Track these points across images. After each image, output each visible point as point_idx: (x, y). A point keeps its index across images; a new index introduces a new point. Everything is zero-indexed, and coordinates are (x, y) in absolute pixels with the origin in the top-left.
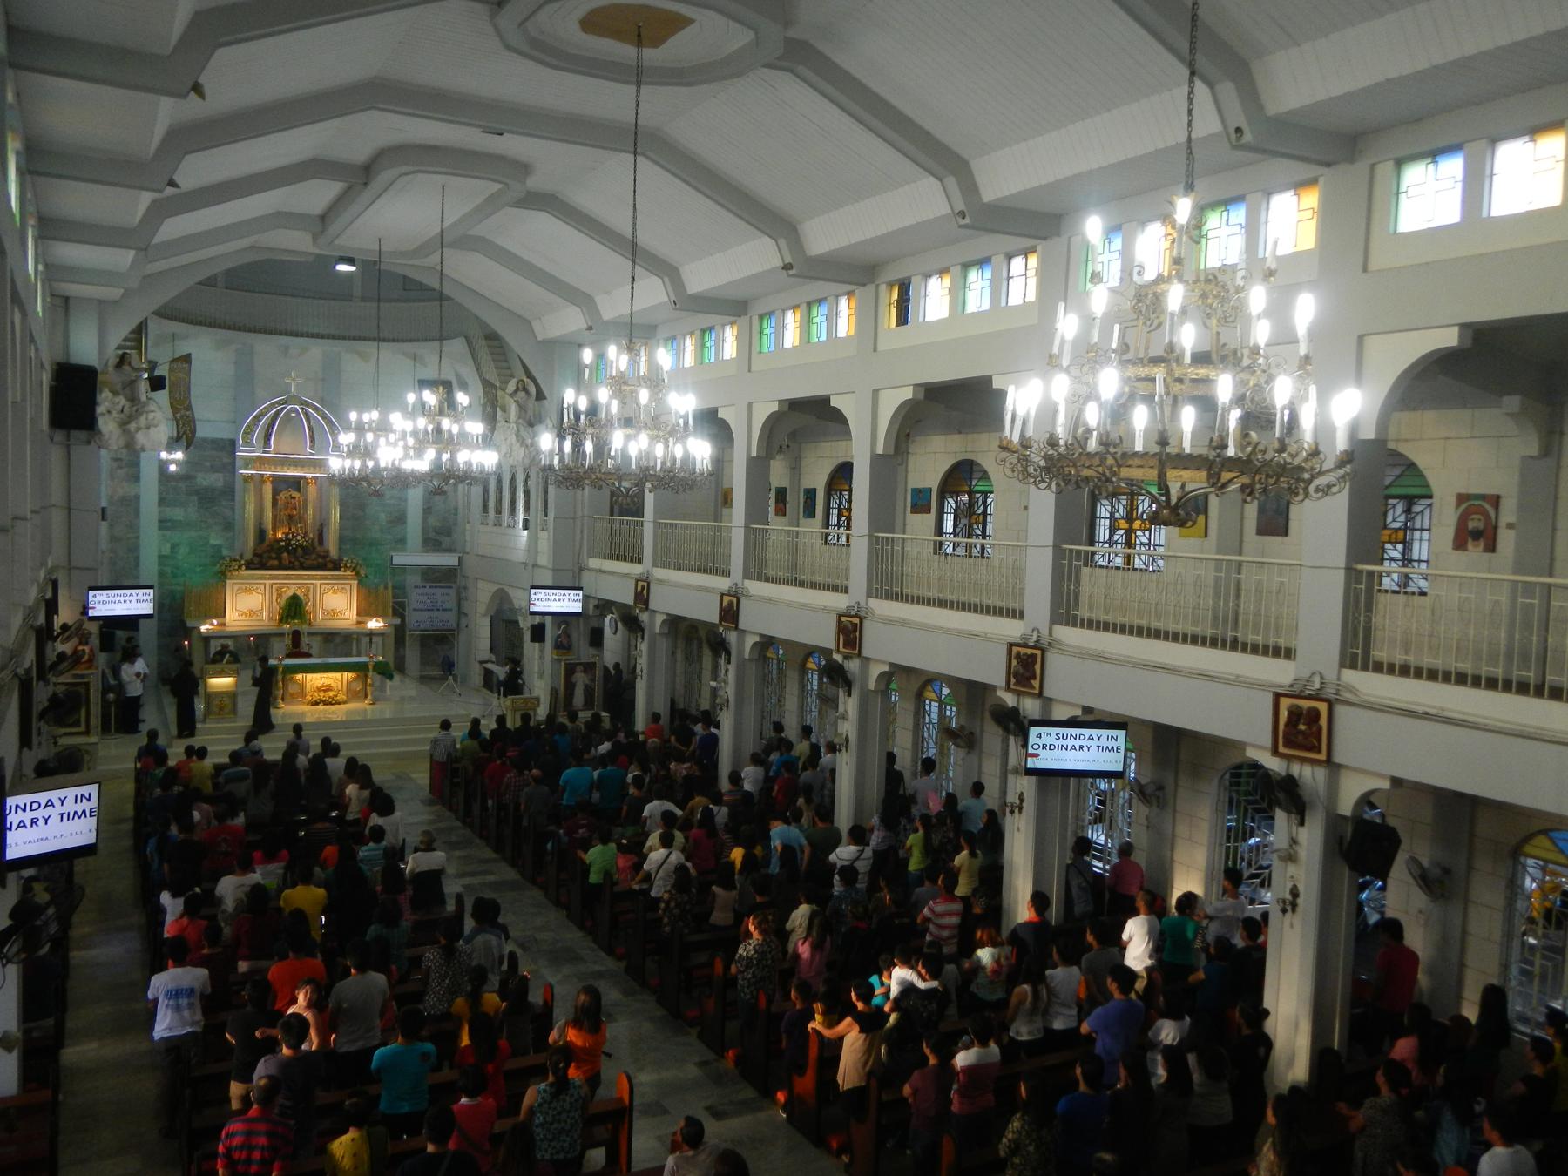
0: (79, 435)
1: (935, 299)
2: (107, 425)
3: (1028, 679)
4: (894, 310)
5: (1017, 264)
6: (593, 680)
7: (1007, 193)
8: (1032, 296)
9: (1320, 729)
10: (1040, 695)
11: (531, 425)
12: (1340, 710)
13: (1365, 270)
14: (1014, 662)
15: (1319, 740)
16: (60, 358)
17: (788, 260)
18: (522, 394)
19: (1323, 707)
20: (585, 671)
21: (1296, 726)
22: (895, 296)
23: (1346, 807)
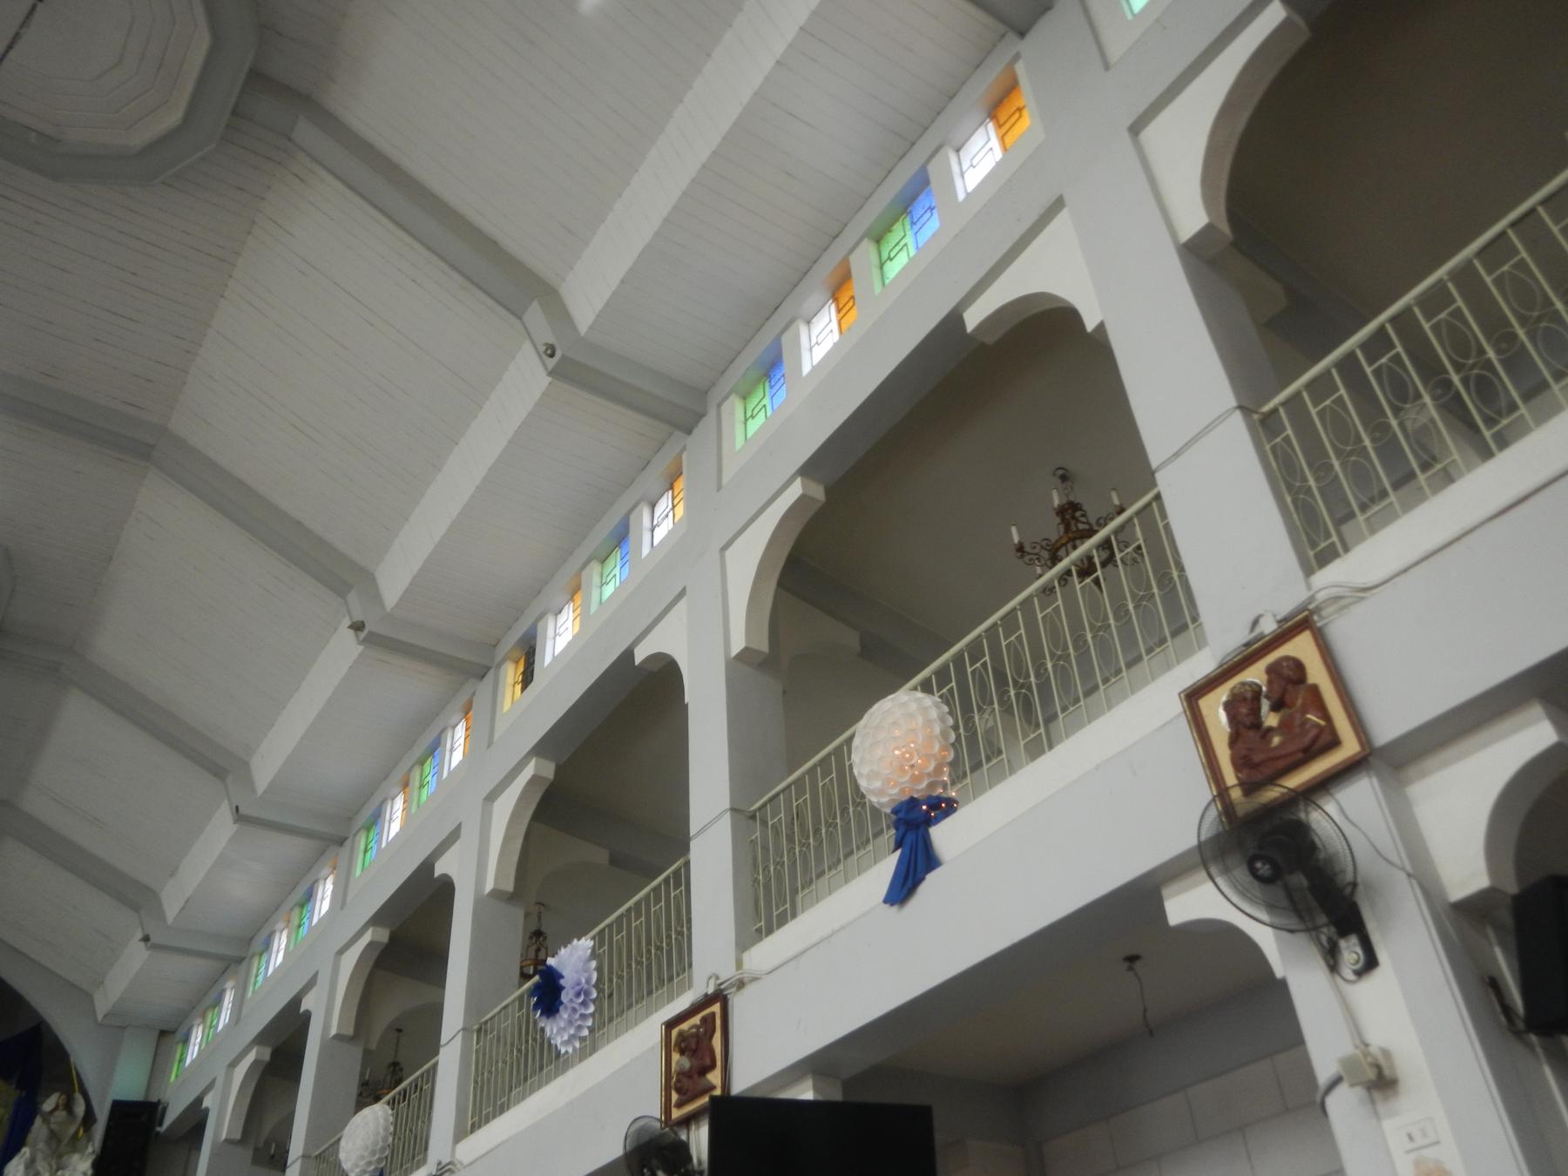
3: (705, 1070)
4: (519, 687)
5: (664, 504)
7: (607, 294)
8: (680, 511)
9: (1315, 691)
11: (60, 1157)
12: (1341, 630)
13: (1107, 67)
14: (676, 1057)
15: (1326, 716)
17: (358, 617)
18: (61, 1114)
19: (1302, 647)
21: (1257, 725)
22: (521, 669)
23: (1466, 869)
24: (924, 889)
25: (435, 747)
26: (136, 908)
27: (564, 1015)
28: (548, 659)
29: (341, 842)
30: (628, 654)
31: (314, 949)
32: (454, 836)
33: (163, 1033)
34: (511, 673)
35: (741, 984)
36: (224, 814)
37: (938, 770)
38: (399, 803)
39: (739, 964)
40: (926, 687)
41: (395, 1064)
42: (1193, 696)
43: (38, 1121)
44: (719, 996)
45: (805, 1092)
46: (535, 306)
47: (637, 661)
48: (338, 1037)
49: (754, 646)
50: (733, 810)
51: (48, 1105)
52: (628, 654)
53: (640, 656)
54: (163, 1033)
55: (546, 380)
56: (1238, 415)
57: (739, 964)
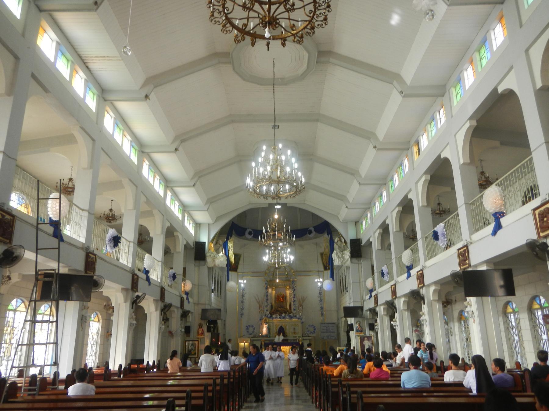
0: (202, 262)
1: (424, 142)
2: (209, 259)
3: (465, 261)
6: (372, 344)
10: (470, 266)
13: (521, 26)
16: (197, 241)
18: (339, 242)
20: (368, 340)
24: (497, 234)
25: (401, 164)
26: (343, 200)
27: (440, 241)
28: (423, 149)
29: (385, 184)
30: (439, 156)
31: (384, 208)
32: (410, 190)
33: (356, 222)
34: (415, 149)
35: (471, 243)
36: (355, 183)
37: (501, 206)
38: (396, 175)
39: (470, 238)
40: (498, 185)
41: (413, 230)
42: (535, 210)
43: (335, 244)
44: (466, 246)
45: (484, 268)
46: (395, 81)
47: (442, 157)
48: (396, 231)
49: (466, 162)
50: (465, 203)
51: (336, 240)
52: (439, 156)
53: (442, 157)
54: (356, 222)
55: (402, 98)
56: (544, 145)
57: (470, 238)
